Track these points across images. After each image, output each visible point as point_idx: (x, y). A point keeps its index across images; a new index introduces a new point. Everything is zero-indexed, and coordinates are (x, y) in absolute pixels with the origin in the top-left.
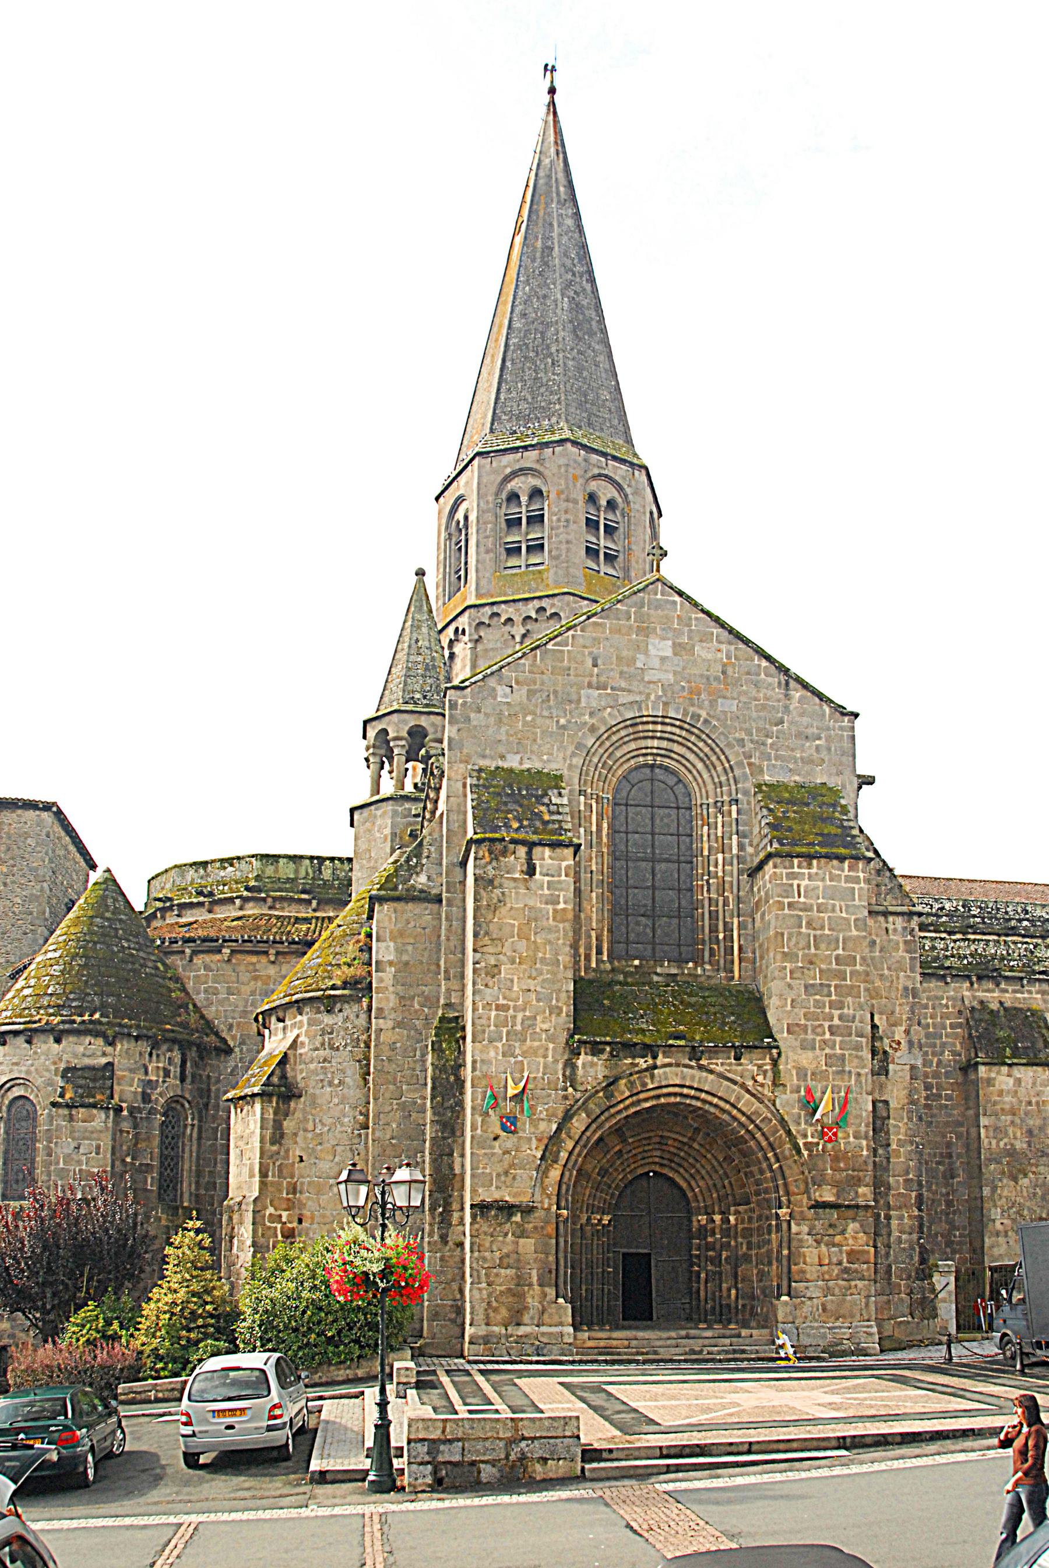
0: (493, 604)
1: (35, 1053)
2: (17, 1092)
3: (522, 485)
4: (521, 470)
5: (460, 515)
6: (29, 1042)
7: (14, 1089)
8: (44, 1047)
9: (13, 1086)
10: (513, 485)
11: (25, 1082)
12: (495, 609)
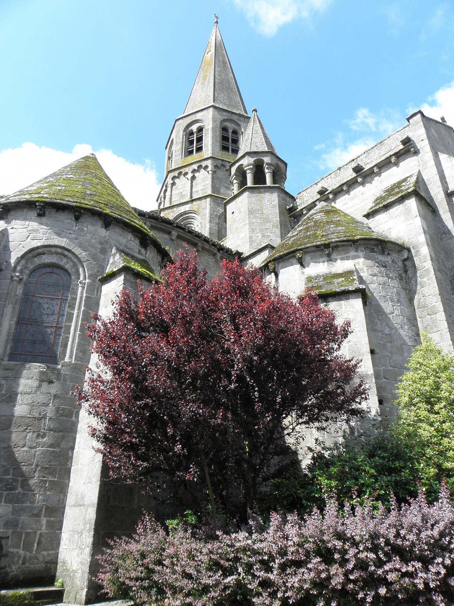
0: (223, 160)
1: (82, 230)
2: (47, 259)
3: (231, 126)
4: (231, 120)
6: (77, 218)
7: (44, 256)
8: (91, 228)
9: (44, 254)
10: (228, 124)
11: (63, 251)
12: (224, 163)
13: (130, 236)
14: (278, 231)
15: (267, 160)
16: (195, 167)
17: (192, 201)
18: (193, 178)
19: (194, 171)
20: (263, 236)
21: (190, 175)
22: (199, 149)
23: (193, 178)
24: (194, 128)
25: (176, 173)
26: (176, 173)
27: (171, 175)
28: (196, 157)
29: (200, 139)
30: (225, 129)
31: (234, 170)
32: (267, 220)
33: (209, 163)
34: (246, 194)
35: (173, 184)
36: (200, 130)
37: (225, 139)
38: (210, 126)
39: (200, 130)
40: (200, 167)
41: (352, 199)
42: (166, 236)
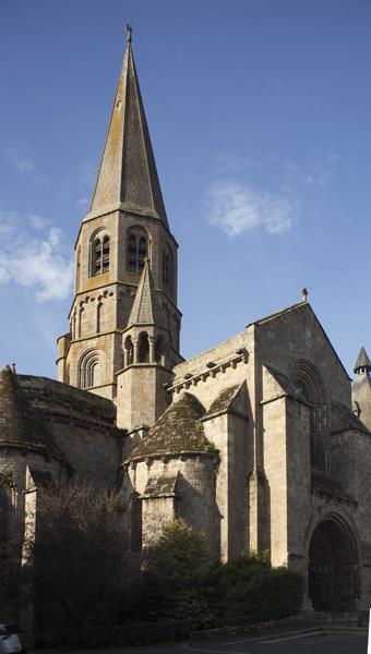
5: (100, 236)
10: (135, 232)
13: (38, 457)
14: (153, 410)
15: (150, 332)
16: (101, 292)
17: (99, 336)
18: (100, 304)
19: (100, 298)
20: (142, 414)
21: (97, 302)
22: (106, 265)
23: (100, 304)
24: (100, 236)
25: (83, 297)
26: (83, 297)
27: (79, 299)
28: (101, 279)
29: (107, 251)
30: (132, 237)
31: (125, 336)
32: (146, 399)
33: (113, 289)
34: (130, 370)
35: (82, 310)
36: (107, 239)
37: (131, 250)
38: (116, 239)
39: (107, 239)
40: (106, 293)
41: (207, 388)
42: (66, 426)
